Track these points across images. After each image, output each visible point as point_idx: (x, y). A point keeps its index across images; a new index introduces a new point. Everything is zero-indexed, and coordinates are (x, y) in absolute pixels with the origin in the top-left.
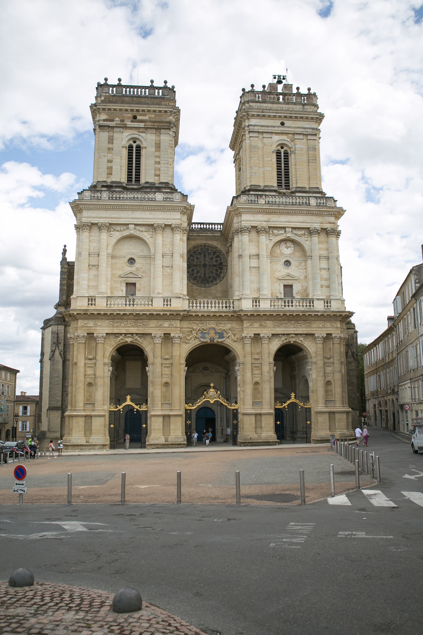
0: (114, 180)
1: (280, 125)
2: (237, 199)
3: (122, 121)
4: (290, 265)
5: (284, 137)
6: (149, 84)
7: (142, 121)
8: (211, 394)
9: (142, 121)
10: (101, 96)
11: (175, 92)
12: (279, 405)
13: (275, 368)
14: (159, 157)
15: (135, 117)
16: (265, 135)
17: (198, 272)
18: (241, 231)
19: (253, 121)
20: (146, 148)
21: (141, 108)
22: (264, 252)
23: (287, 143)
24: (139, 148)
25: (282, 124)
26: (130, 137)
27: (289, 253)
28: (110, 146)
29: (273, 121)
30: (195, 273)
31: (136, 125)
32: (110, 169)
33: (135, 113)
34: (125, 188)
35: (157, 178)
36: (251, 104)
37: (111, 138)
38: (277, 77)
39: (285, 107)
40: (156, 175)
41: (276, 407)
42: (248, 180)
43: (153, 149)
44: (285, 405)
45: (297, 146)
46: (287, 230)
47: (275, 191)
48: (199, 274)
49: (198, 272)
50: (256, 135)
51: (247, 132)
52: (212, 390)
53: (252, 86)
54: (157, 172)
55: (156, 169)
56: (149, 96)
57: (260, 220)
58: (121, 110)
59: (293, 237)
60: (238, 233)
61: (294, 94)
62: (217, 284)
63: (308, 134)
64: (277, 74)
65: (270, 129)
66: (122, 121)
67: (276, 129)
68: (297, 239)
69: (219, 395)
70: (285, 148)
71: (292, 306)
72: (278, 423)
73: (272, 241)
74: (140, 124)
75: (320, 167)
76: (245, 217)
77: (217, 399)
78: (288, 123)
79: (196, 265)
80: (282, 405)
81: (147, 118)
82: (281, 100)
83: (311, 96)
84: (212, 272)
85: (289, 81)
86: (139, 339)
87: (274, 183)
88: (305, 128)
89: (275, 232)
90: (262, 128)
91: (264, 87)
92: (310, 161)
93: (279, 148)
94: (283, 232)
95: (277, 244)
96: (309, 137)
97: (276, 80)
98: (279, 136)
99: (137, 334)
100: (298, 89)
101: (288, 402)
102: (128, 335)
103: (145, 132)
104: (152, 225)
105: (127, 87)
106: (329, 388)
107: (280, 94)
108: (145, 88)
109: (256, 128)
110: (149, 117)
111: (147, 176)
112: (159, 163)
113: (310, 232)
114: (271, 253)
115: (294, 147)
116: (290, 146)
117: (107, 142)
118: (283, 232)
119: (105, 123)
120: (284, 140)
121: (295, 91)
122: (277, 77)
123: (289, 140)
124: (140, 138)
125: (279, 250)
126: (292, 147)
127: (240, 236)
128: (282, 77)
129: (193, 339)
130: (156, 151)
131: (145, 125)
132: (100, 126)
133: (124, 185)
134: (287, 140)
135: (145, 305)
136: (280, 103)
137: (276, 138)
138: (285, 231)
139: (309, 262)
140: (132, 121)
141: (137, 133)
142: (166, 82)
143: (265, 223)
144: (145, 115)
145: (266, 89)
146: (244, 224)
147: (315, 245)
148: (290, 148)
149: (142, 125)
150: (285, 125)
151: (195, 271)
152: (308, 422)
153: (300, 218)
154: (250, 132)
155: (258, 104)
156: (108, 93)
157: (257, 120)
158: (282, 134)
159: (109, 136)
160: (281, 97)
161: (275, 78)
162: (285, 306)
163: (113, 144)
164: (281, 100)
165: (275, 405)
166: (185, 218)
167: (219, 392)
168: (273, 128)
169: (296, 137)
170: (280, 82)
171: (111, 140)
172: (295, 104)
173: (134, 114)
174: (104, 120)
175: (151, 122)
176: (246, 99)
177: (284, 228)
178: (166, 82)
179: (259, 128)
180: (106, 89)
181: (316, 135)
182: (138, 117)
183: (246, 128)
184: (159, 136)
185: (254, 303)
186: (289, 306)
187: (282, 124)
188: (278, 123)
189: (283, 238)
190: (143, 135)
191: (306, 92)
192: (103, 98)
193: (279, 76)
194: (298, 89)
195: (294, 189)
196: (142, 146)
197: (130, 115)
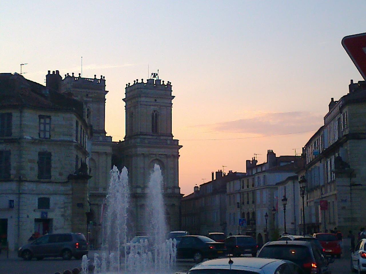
1: (154, 101)
5: (156, 107)
7: (91, 97)
9: (91, 97)
18: (137, 155)
19: (143, 99)
21: (91, 91)
25: (156, 100)
36: (141, 90)
42: (139, 129)
47: (152, 135)
50: (144, 106)
57: (145, 150)
58: (81, 91)
59: (159, 158)
64: (153, 73)
65: (150, 104)
70: (156, 112)
76: (139, 149)
83: (169, 85)
87: (150, 131)
93: (153, 112)
96: (168, 108)
97: (153, 76)
100: (163, 82)
104: (98, 152)
116: (158, 111)
121: (162, 83)
122: (153, 74)
128: (156, 74)
135: (95, 191)
137: (152, 107)
139: (166, 170)
146: (138, 153)
148: (158, 112)
150: (157, 101)
153: (163, 150)
154: (141, 105)
182: (89, 95)
183: (139, 102)
187: (156, 100)
188: (153, 100)
193: (155, 74)
194: (163, 82)
195: (159, 134)
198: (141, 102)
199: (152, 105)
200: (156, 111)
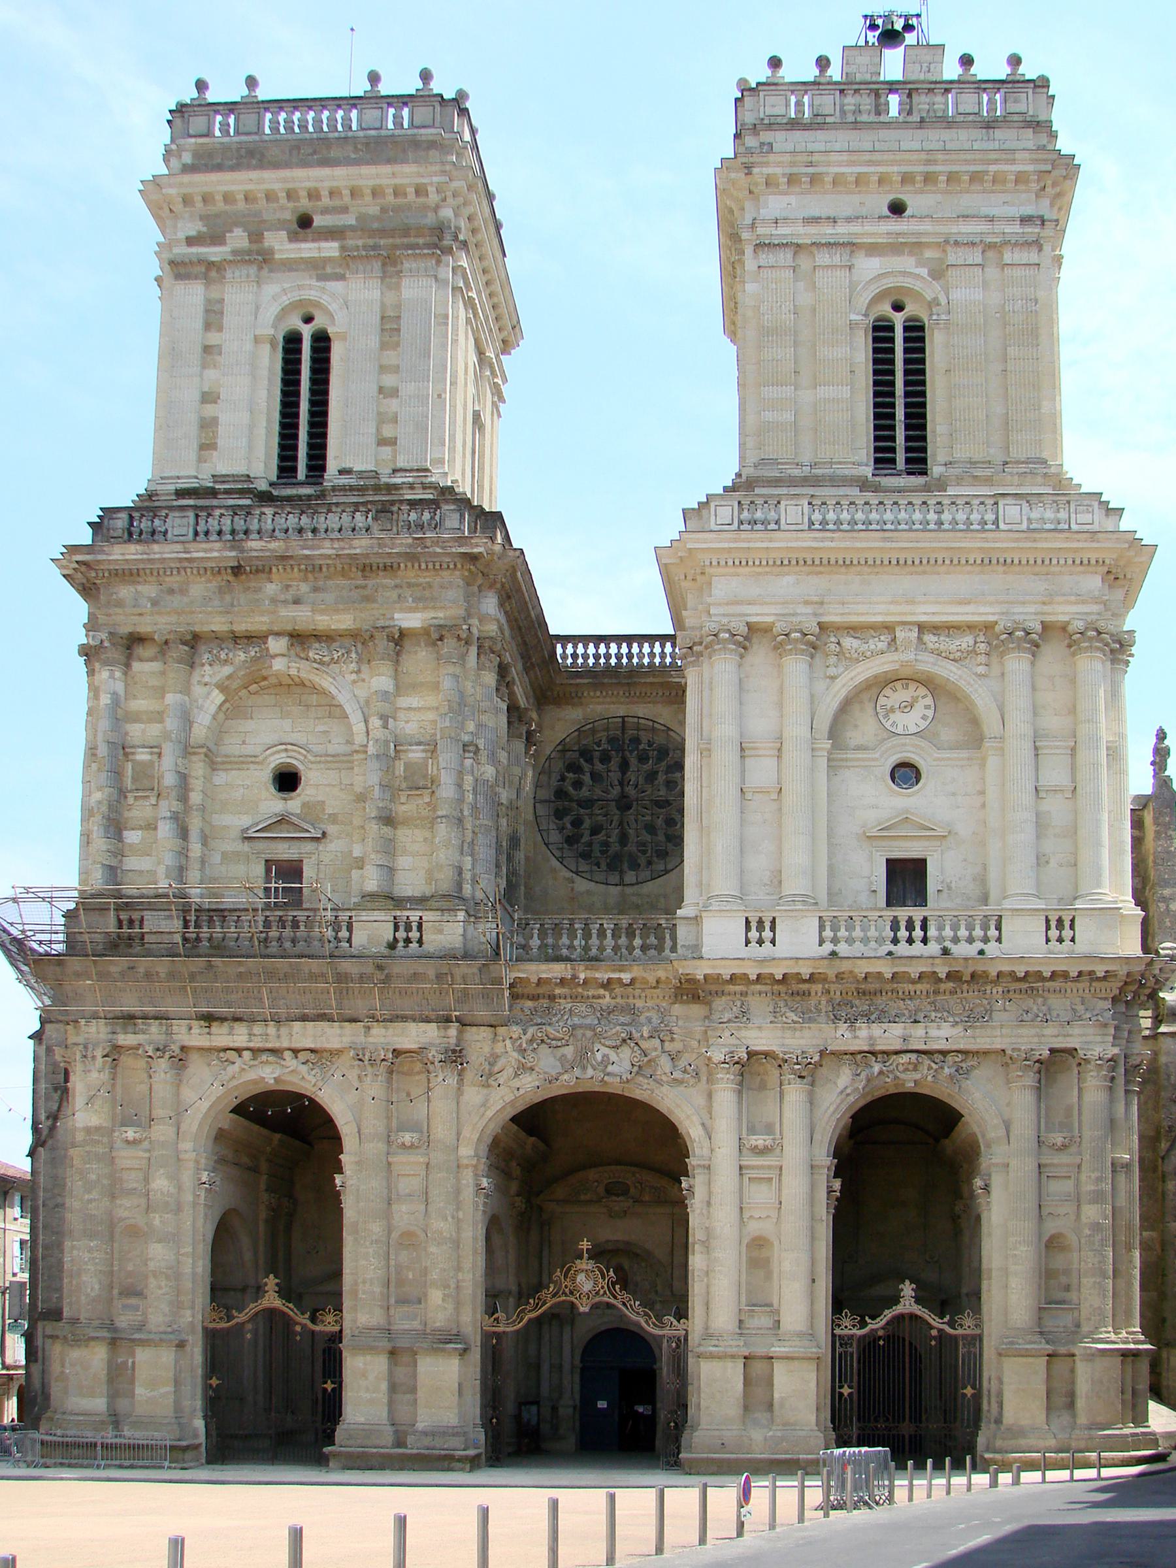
0: (223, 469)
1: (886, 212)
2: (700, 517)
3: (256, 237)
4: (917, 782)
5: (906, 263)
6: (360, 87)
8: (581, 1277)
10: (180, 149)
11: (464, 112)
12: (846, 1322)
13: (837, 1184)
14: (396, 369)
15: (305, 222)
16: (823, 258)
17: (595, 831)
19: (775, 205)
20: (343, 337)
22: (797, 731)
23: (918, 286)
24: (322, 342)
25: (897, 209)
26: (285, 300)
27: (913, 729)
28: (214, 338)
29: (856, 199)
30: (587, 833)
31: (308, 249)
32: (208, 425)
33: (304, 204)
34: (265, 498)
35: (387, 450)
36: (766, 136)
37: (216, 307)
38: (880, 22)
39: (911, 140)
40: (382, 442)
41: (837, 1331)
43: (374, 341)
44: (876, 1325)
45: (955, 295)
46: (900, 634)
48: (601, 837)
49: (595, 831)
51: (749, 250)
52: (585, 1264)
53: (775, 63)
54: (387, 432)
55: (382, 419)
56: (361, 134)
60: (700, 654)
61: (947, 87)
62: (667, 872)
63: (1006, 243)
66: (256, 237)
67: (869, 228)
68: (944, 674)
69: (614, 1284)
71: (925, 941)
72: (846, 1391)
73: (839, 682)
74: (324, 244)
75: (1053, 375)
77: (606, 1299)
78: (913, 203)
79: (587, 803)
80: (863, 1324)
81: (350, 220)
82: (894, 111)
84: (651, 829)
85: (934, 30)
86: (304, 1069)
88: (991, 219)
89: (848, 642)
90: (812, 230)
91: (823, 63)
92: (1011, 351)
94: (882, 646)
95: (865, 696)
96: (1008, 257)
98: (885, 259)
99: (296, 1052)
100: (967, 61)
101: (888, 1314)
102: (264, 1057)
103: (341, 277)
105: (279, 105)
106: (1059, 1262)
107: (893, 87)
108: (353, 102)
109: (783, 230)
110: (361, 218)
111: (349, 449)
112: (394, 393)
113: (996, 639)
114: (835, 732)
115: (943, 301)
117: (199, 324)
118: (882, 646)
119: (194, 250)
120: (904, 274)
123: (924, 272)
124: (325, 300)
125: (872, 721)
126: (935, 302)
127: (705, 666)
129: (509, 1071)
130: (384, 346)
131: (343, 248)
132: (172, 263)
133: (263, 486)
134: (918, 271)
136: (888, 125)
137: (869, 266)
138: (894, 639)
140: (293, 238)
141: (314, 282)
142: (426, 76)
143: (809, 610)
144: (345, 210)
145: (835, 72)
147: (1008, 693)
149: (331, 249)
151: (587, 823)
152: (969, 1391)
155: (798, 135)
156: (209, 134)
157: (792, 199)
158: (895, 248)
159: (208, 301)
160: (894, 100)
161: (873, 27)
162: (895, 941)
163: (220, 329)
164: (894, 111)
165: (835, 1324)
166: (490, 604)
167: (611, 1273)
168: (855, 228)
169: (954, 256)
170: (890, 37)
171: (213, 317)
172: (948, 123)
173: (302, 210)
174: (190, 241)
175: (373, 233)
176: (749, 118)
177: (889, 628)
178: (426, 76)
179: (800, 229)
180: (197, 123)
181: (1037, 244)
182: (318, 221)
184: (398, 287)
185: (754, 928)
186: (910, 941)
189: (886, 668)
190: (336, 286)
191: (1001, 71)
192: (187, 158)
194: (967, 61)
196: (331, 331)
197: (288, 215)
198: (760, 230)
199: (873, 249)
200: (917, 296)
